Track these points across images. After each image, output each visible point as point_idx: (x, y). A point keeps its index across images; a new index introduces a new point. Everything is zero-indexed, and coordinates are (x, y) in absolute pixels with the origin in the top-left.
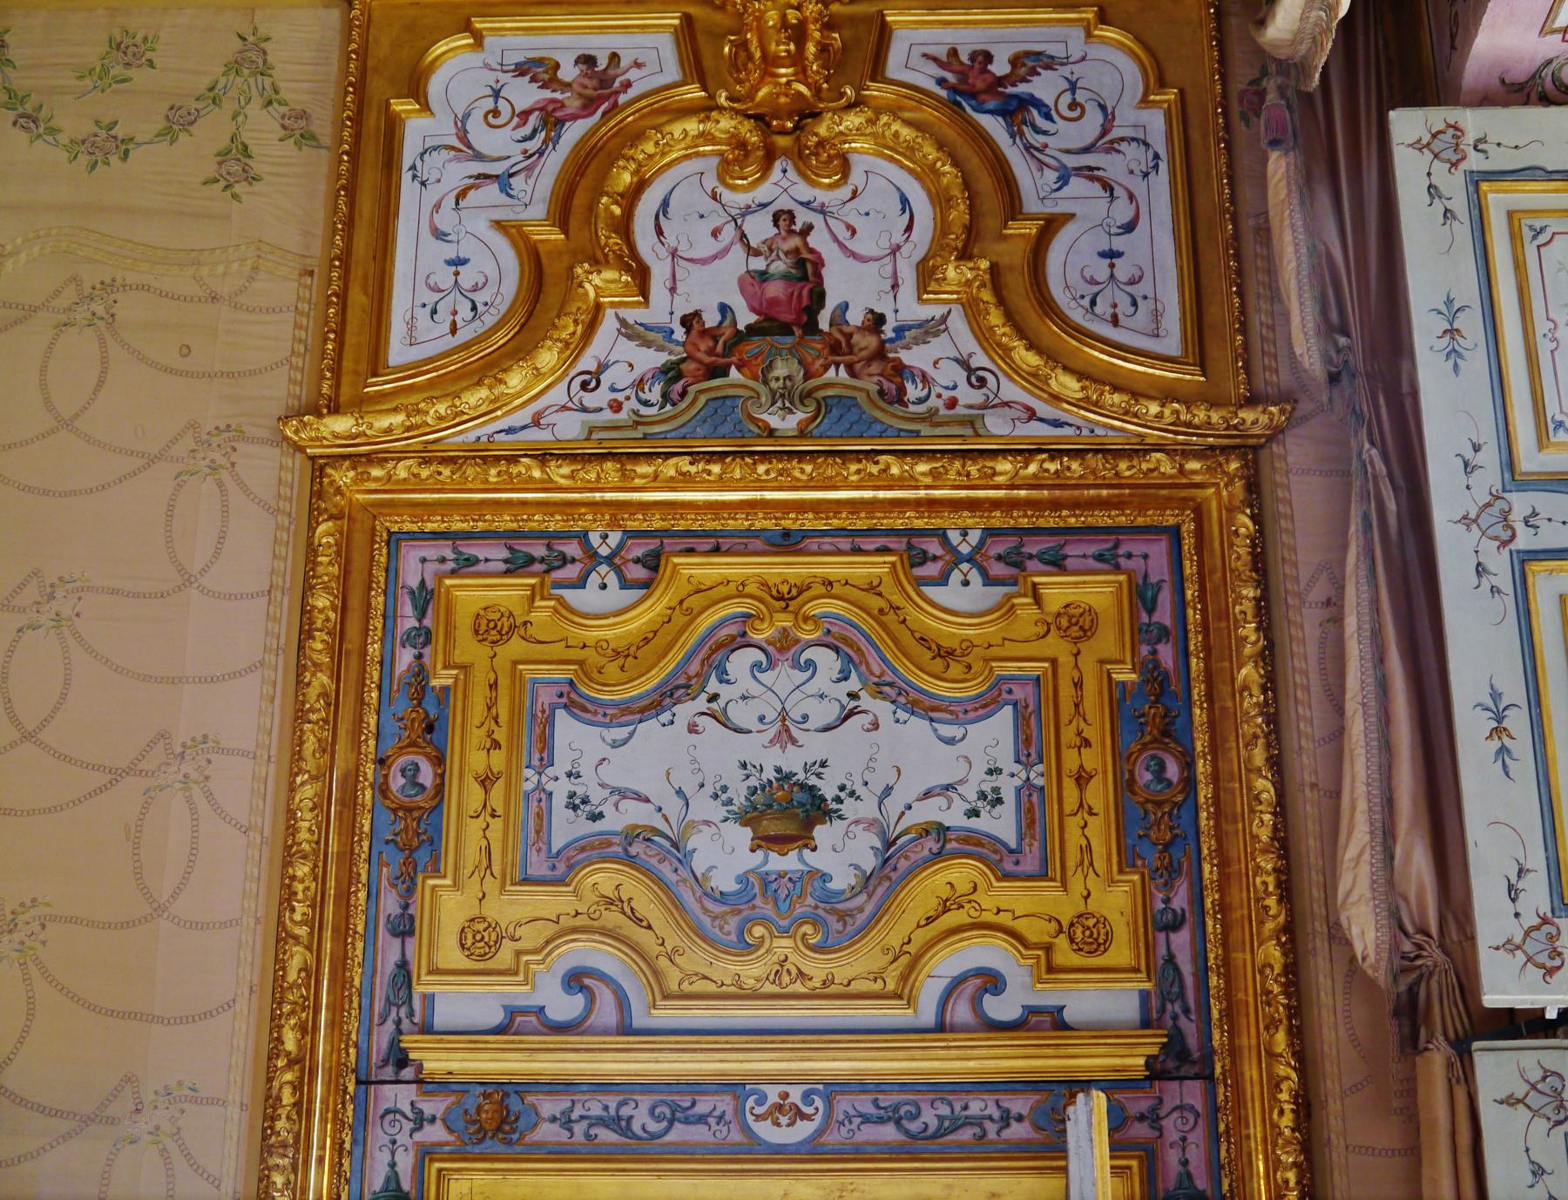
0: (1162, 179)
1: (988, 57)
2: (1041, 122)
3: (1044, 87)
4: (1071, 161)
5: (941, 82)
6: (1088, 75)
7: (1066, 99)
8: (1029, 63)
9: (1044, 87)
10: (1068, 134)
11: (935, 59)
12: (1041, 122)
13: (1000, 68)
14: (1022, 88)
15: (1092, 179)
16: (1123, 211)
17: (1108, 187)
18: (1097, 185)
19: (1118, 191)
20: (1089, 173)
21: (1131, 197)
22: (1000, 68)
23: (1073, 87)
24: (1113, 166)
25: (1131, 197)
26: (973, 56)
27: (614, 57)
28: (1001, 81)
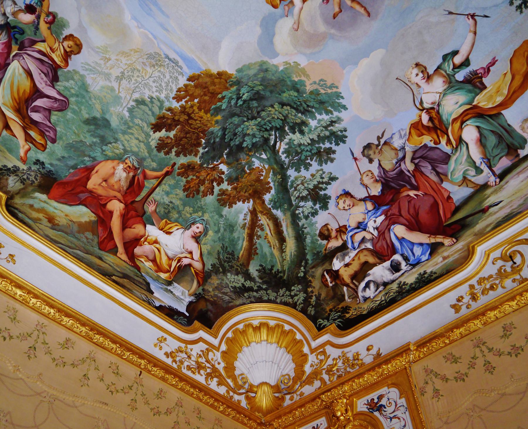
0: (407, 413)
1: (373, 399)
2: (385, 409)
3: (384, 402)
4: (392, 415)
5: (367, 408)
6: (390, 396)
7: (388, 402)
8: (380, 397)
9: (384, 402)
10: (389, 410)
11: (365, 404)
12: (385, 409)
13: (376, 401)
14: (380, 403)
15: (396, 418)
16: (403, 423)
17: (399, 419)
18: (397, 419)
19: (402, 419)
20: (395, 417)
21: (404, 419)
22: (376, 401)
23: (389, 399)
24: (398, 413)
25: (404, 419)
26: (371, 400)
27: (317, 425)
28: (377, 403)
